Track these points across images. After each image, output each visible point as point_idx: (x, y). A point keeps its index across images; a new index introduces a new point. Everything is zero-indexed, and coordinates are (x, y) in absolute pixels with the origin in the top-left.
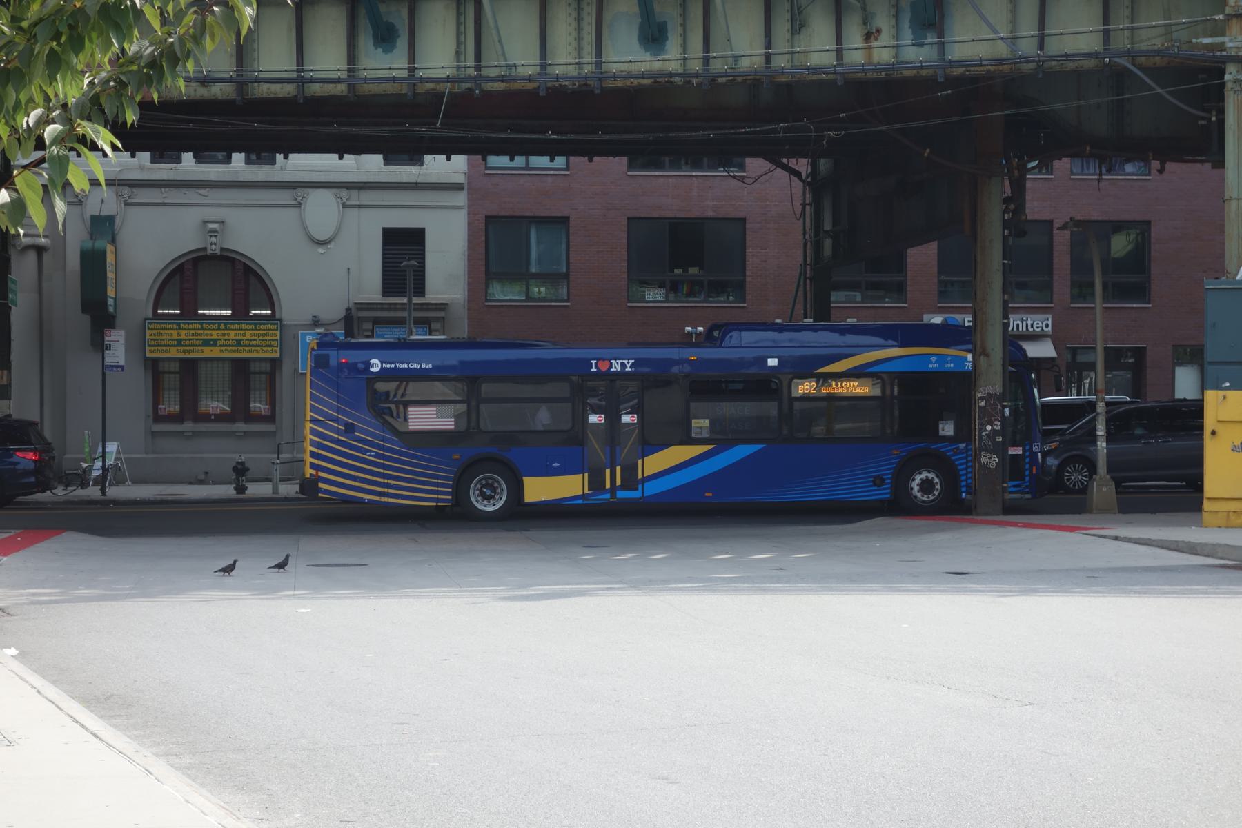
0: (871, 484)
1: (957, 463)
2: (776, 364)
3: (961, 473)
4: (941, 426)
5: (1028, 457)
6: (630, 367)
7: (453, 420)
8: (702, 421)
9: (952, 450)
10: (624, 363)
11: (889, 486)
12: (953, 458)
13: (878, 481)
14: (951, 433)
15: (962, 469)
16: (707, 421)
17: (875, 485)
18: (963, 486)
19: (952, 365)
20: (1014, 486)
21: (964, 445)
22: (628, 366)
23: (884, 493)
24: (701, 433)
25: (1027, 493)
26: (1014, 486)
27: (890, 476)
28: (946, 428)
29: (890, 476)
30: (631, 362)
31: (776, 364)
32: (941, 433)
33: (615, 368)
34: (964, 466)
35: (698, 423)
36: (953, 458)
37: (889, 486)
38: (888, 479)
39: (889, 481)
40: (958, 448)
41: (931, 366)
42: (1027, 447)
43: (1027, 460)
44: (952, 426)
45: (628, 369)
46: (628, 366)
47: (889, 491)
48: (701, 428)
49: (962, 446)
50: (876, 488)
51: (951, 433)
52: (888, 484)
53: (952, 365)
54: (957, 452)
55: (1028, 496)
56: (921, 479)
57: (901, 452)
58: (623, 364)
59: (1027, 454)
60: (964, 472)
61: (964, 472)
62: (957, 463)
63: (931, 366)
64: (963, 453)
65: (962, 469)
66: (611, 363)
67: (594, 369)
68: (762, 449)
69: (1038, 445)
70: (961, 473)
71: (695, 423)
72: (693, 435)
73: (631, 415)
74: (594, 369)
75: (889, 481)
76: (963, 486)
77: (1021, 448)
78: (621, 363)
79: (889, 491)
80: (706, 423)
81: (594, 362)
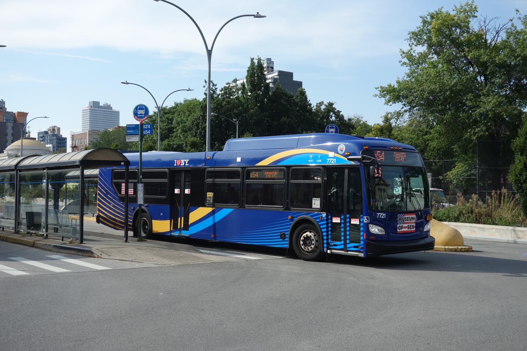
4: (313, 201)
6: (187, 164)
7: (133, 190)
13: (283, 236)
17: (281, 238)
20: (355, 247)
22: (187, 162)
23: (285, 244)
25: (362, 252)
26: (355, 247)
28: (316, 203)
30: (188, 160)
33: (182, 164)
45: (186, 165)
46: (187, 162)
50: (281, 240)
56: (311, 236)
58: (185, 161)
59: (362, 224)
64: (324, 220)
66: (181, 161)
67: (175, 165)
74: (175, 165)
77: (358, 220)
78: (185, 161)
81: (176, 161)
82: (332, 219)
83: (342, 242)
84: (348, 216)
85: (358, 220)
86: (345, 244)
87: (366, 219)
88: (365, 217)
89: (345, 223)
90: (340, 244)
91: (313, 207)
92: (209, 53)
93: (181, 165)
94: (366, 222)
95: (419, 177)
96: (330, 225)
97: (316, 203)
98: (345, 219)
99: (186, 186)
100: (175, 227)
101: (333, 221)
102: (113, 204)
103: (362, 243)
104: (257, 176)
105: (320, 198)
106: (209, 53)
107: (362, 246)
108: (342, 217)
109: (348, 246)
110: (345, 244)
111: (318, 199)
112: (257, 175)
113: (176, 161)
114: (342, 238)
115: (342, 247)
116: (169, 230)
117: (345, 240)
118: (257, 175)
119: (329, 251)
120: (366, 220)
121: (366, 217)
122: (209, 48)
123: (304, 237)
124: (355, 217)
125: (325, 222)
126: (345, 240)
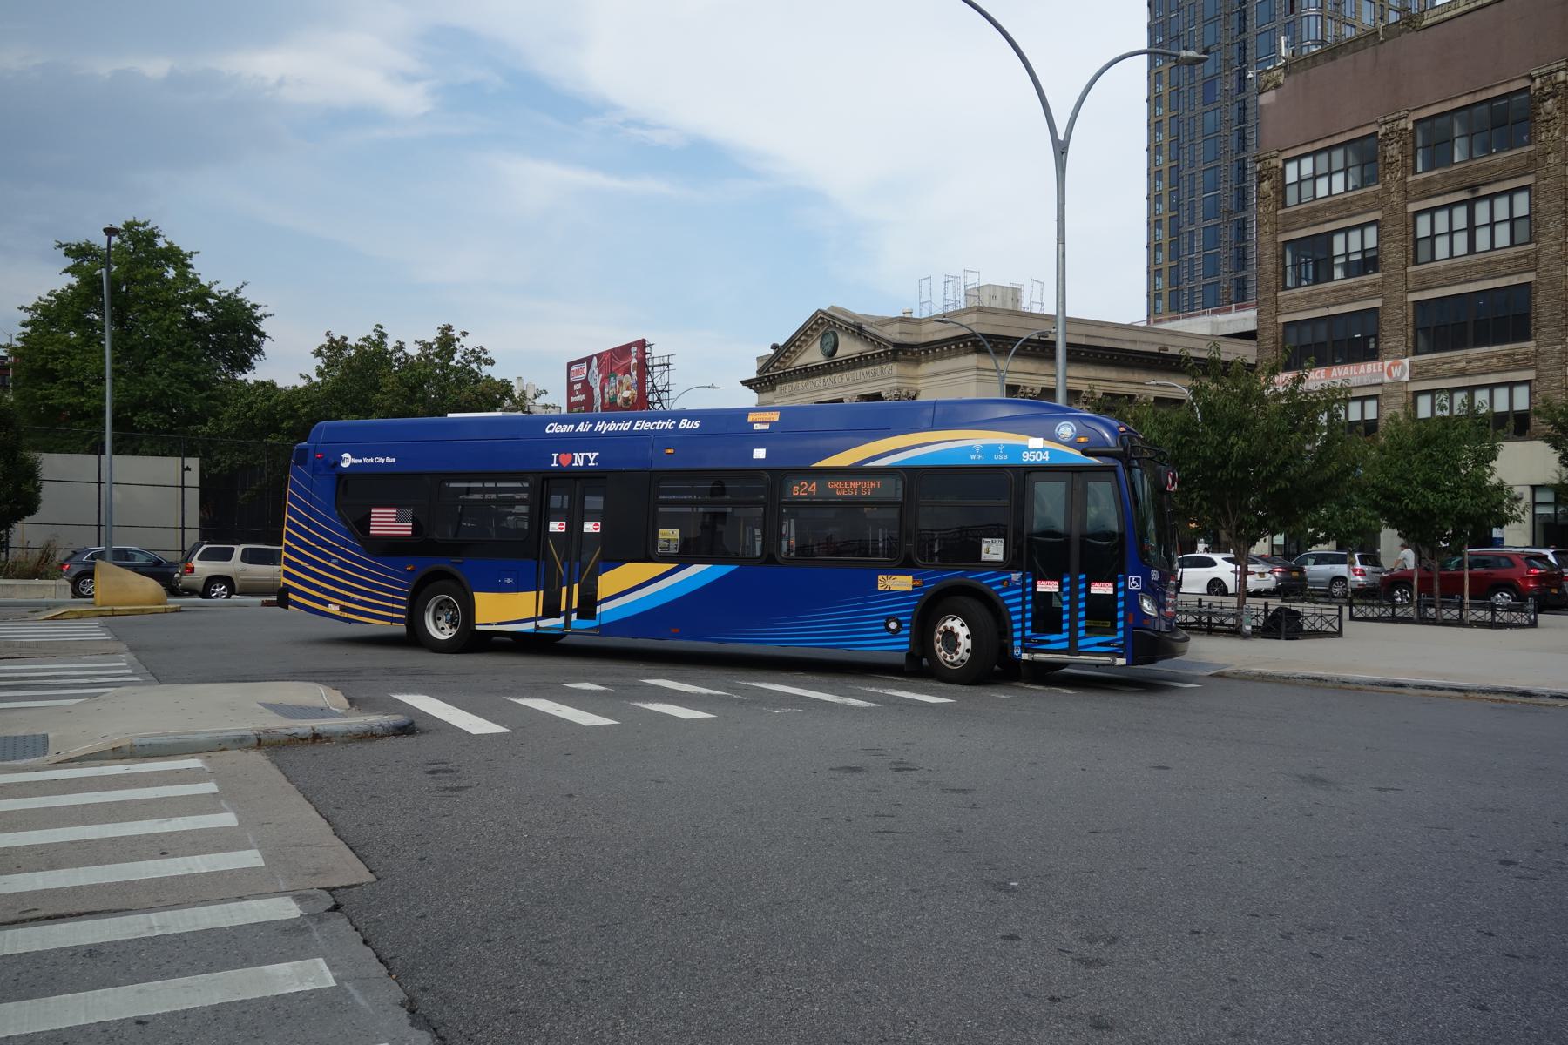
0: (883, 627)
1: (1007, 602)
2: (755, 451)
3: (1014, 618)
4: (984, 546)
5: (1121, 599)
7: (411, 524)
8: (670, 531)
9: (1001, 582)
10: (587, 456)
11: (908, 632)
12: (1002, 595)
14: (1000, 558)
15: (1016, 613)
16: (677, 532)
18: (1017, 639)
19: (1005, 457)
21: (1019, 575)
24: (668, 548)
27: (910, 618)
28: (993, 549)
29: (910, 618)
31: (755, 451)
32: (985, 556)
34: (1019, 608)
35: (666, 534)
36: (1002, 595)
37: (908, 632)
38: (906, 622)
39: (908, 625)
40: (1009, 580)
41: (973, 457)
42: (1120, 585)
43: (1120, 604)
44: (1001, 547)
47: (907, 639)
48: (668, 541)
49: (1016, 576)
50: (887, 634)
51: (1000, 558)
52: (906, 629)
53: (1005, 457)
54: (1010, 585)
55: (1121, 661)
57: (926, 583)
58: (586, 457)
59: (1120, 595)
60: (1019, 617)
61: (1019, 617)
62: (1007, 602)
63: (973, 457)
64: (1016, 588)
65: (1016, 613)
68: (735, 570)
69: (1137, 580)
70: (1014, 618)
71: (663, 534)
72: (660, 550)
73: (594, 523)
75: (908, 625)
76: (1017, 639)
77: (1111, 585)
79: (907, 639)
80: (674, 534)
82: (1036, 584)
83: (1066, 635)
84: (1082, 577)
85: (1111, 585)
86: (1073, 639)
87: (1134, 582)
88: (1131, 579)
89: (1073, 593)
90: (1059, 640)
91: (983, 558)
92: (1061, 149)
93: (575, 464)
94: (1134, 588)
95: (721, 533)
96: (1029, 598)
97: (993, 550)
98: (1074, 583)
99: (1070, 474)
100: (551, 610)
101: (1038, 590)
102: (339, 559)
103: (1120, 634)
104: (814, 490)
105: (1003, 540)
106: (1061, 149)
107: (1122, 642)
108: (1066, 580)
109: (1081, 643)
110: (1073, 639)
111: (997, 540)
112: (813, 488)
113: (557, 457)
114: (1066, 626)
115: (1065, 645)
116: (534, 616)
117: (1073, 630)
118: (813, 488)
119: (1025, 656)
120: (1134, 585)
121: (1134, 578)
122: (1061, 137)
123: (945, 627)
124: (1101, 579)
125: (1020, 591)
126: (1073, 630)
